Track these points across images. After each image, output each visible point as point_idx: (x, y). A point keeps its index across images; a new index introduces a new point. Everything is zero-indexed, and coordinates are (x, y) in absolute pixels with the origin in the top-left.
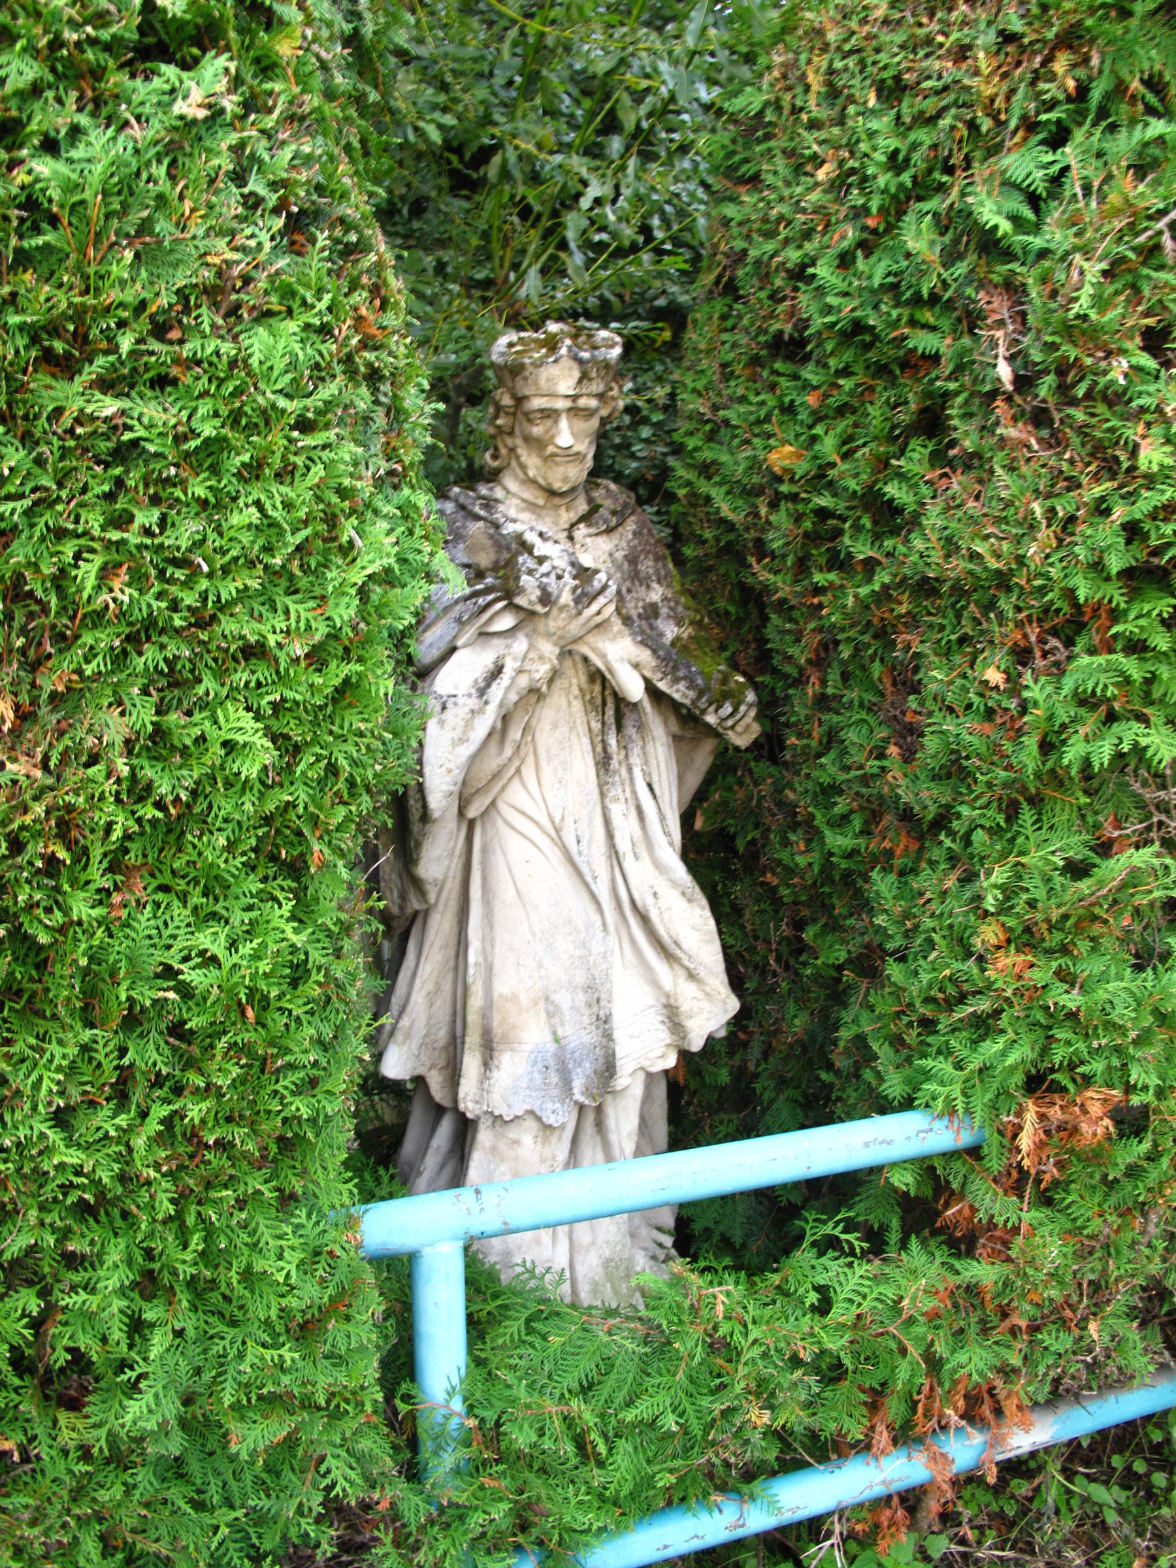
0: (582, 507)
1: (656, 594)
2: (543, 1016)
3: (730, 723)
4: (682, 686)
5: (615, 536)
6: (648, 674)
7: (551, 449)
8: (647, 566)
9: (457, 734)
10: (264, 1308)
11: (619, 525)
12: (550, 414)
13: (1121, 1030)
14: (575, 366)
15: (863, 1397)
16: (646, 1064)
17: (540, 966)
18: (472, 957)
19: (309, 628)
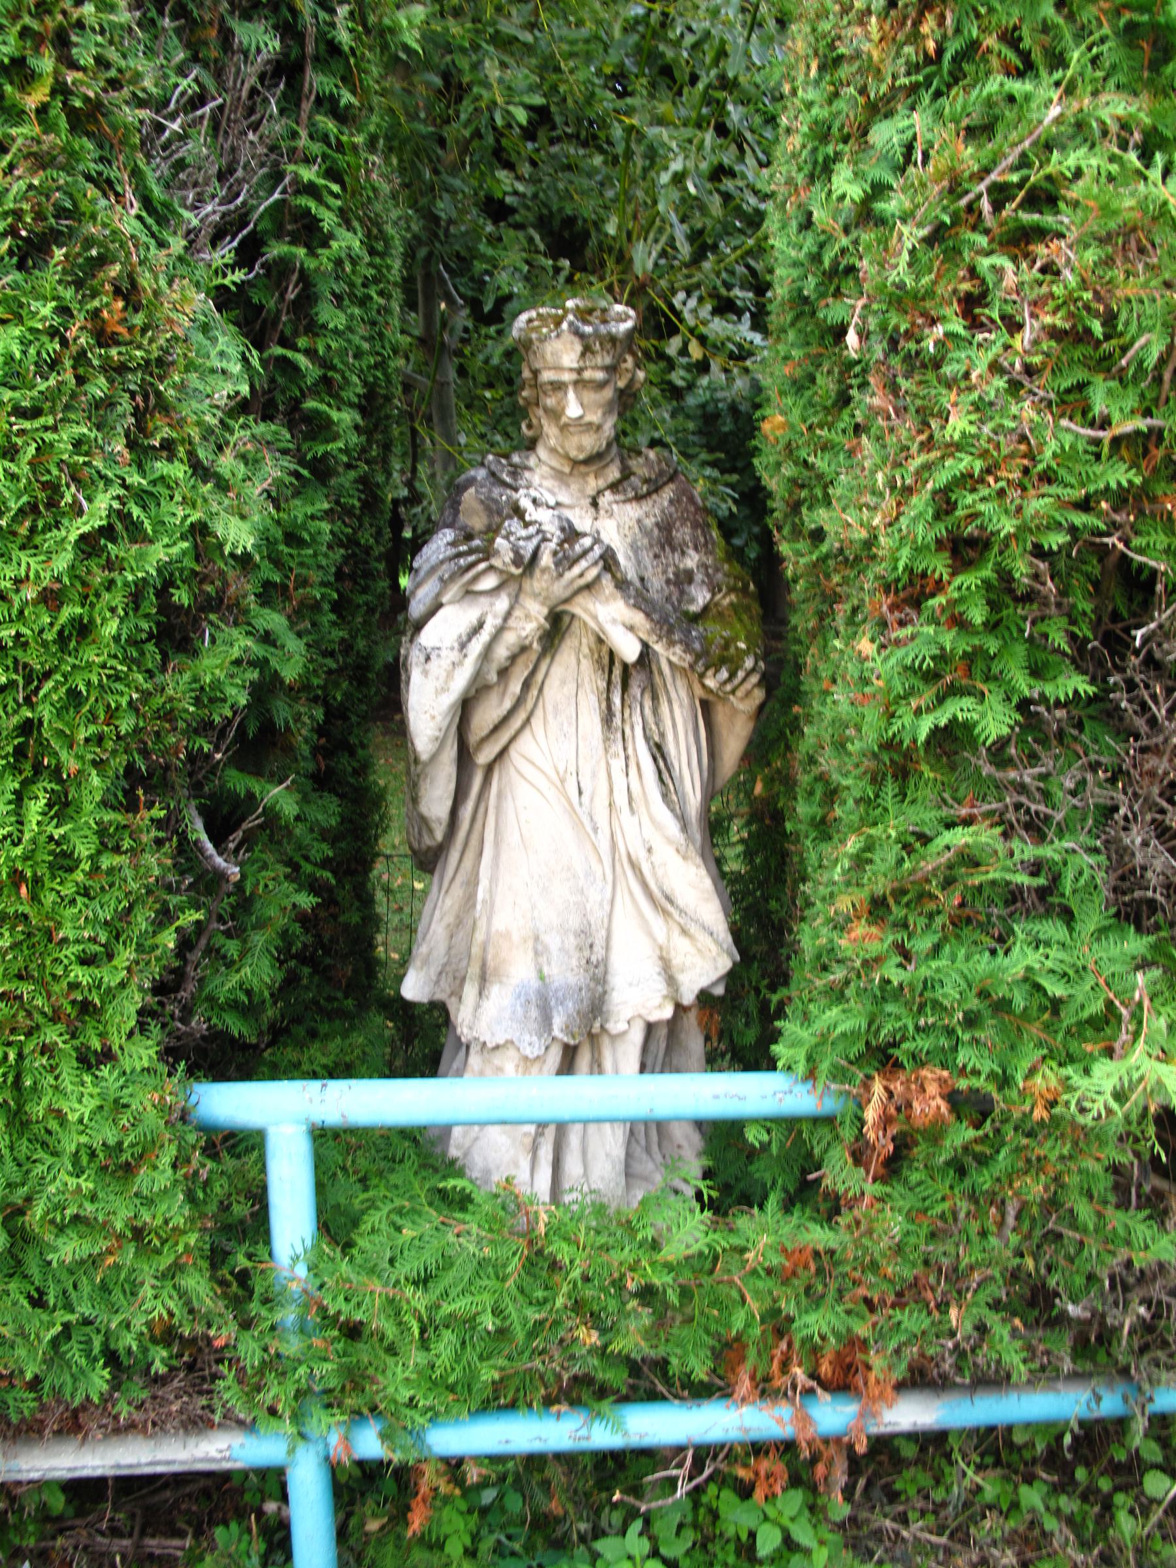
0: (614, 473)
1: (691, 561)
2: (531, 954)
3: (728, 688)
4: (678, 649)
5: (646, 506)
6: (644, 637)
7: (564, 420)
8: (683, 533)
9: (439, 684)
10: (70, 1143)
11: (649, 494)
12: (559, 386)
13: (949, 1012)
15: (711, 1342)
16: (643, 1012)
17: (534, 907)
18: (481, 894)
19: (38, 576)
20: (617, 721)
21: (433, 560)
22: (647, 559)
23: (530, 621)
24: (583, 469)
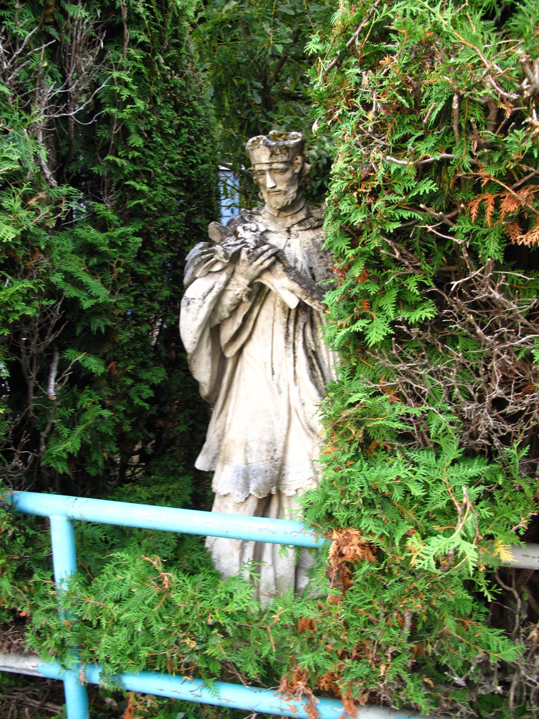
0: (302, 216)
6: (300, 296)
14: (267, 149)
20: (291, 338)
21: (193, 257)
22: (315, 258)
24: (284, 214)
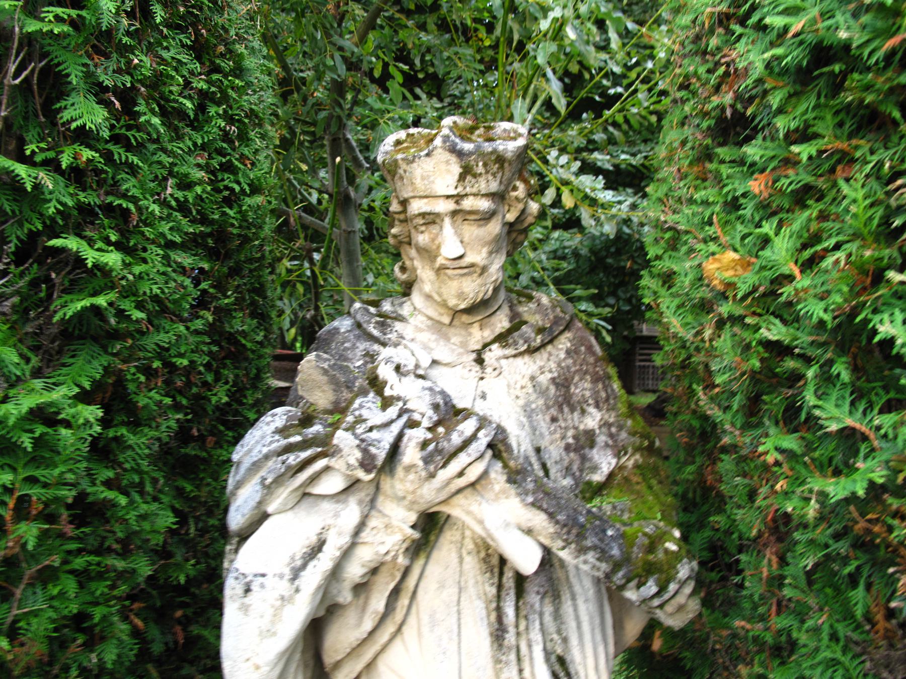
0: (502, 322)
1: (592, 420)
3: (656, 602)
5: (540, 359)
6: (547, 542)
7: (440, 261)
8: (582, 388)
11: (543, 345)
12: (431, 219)
14: (453, 159)
20: (510, 638)
21: (255, 456)
22: (543, 422)
23: (394, 526)
24: (465, 318)
